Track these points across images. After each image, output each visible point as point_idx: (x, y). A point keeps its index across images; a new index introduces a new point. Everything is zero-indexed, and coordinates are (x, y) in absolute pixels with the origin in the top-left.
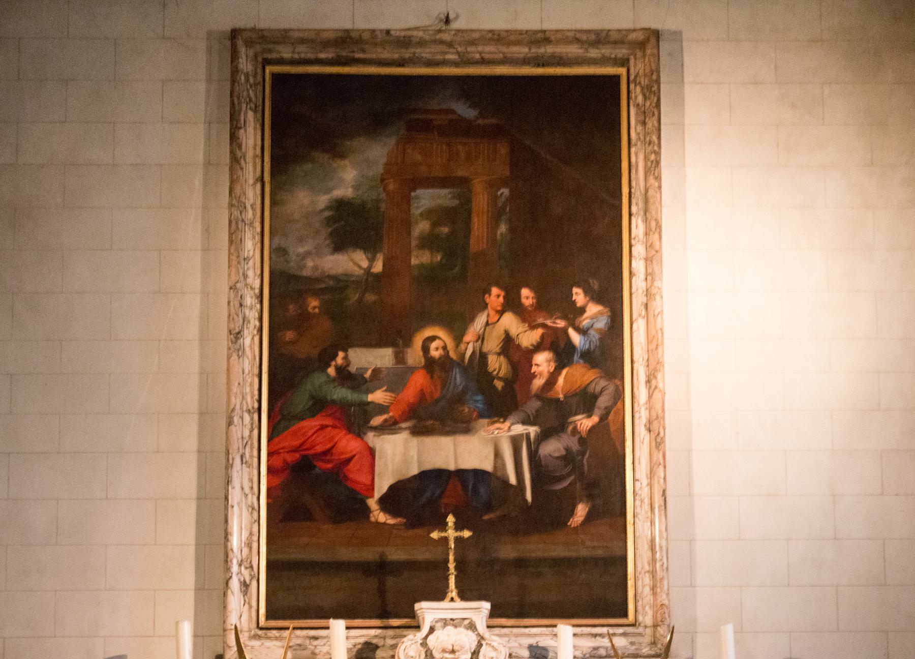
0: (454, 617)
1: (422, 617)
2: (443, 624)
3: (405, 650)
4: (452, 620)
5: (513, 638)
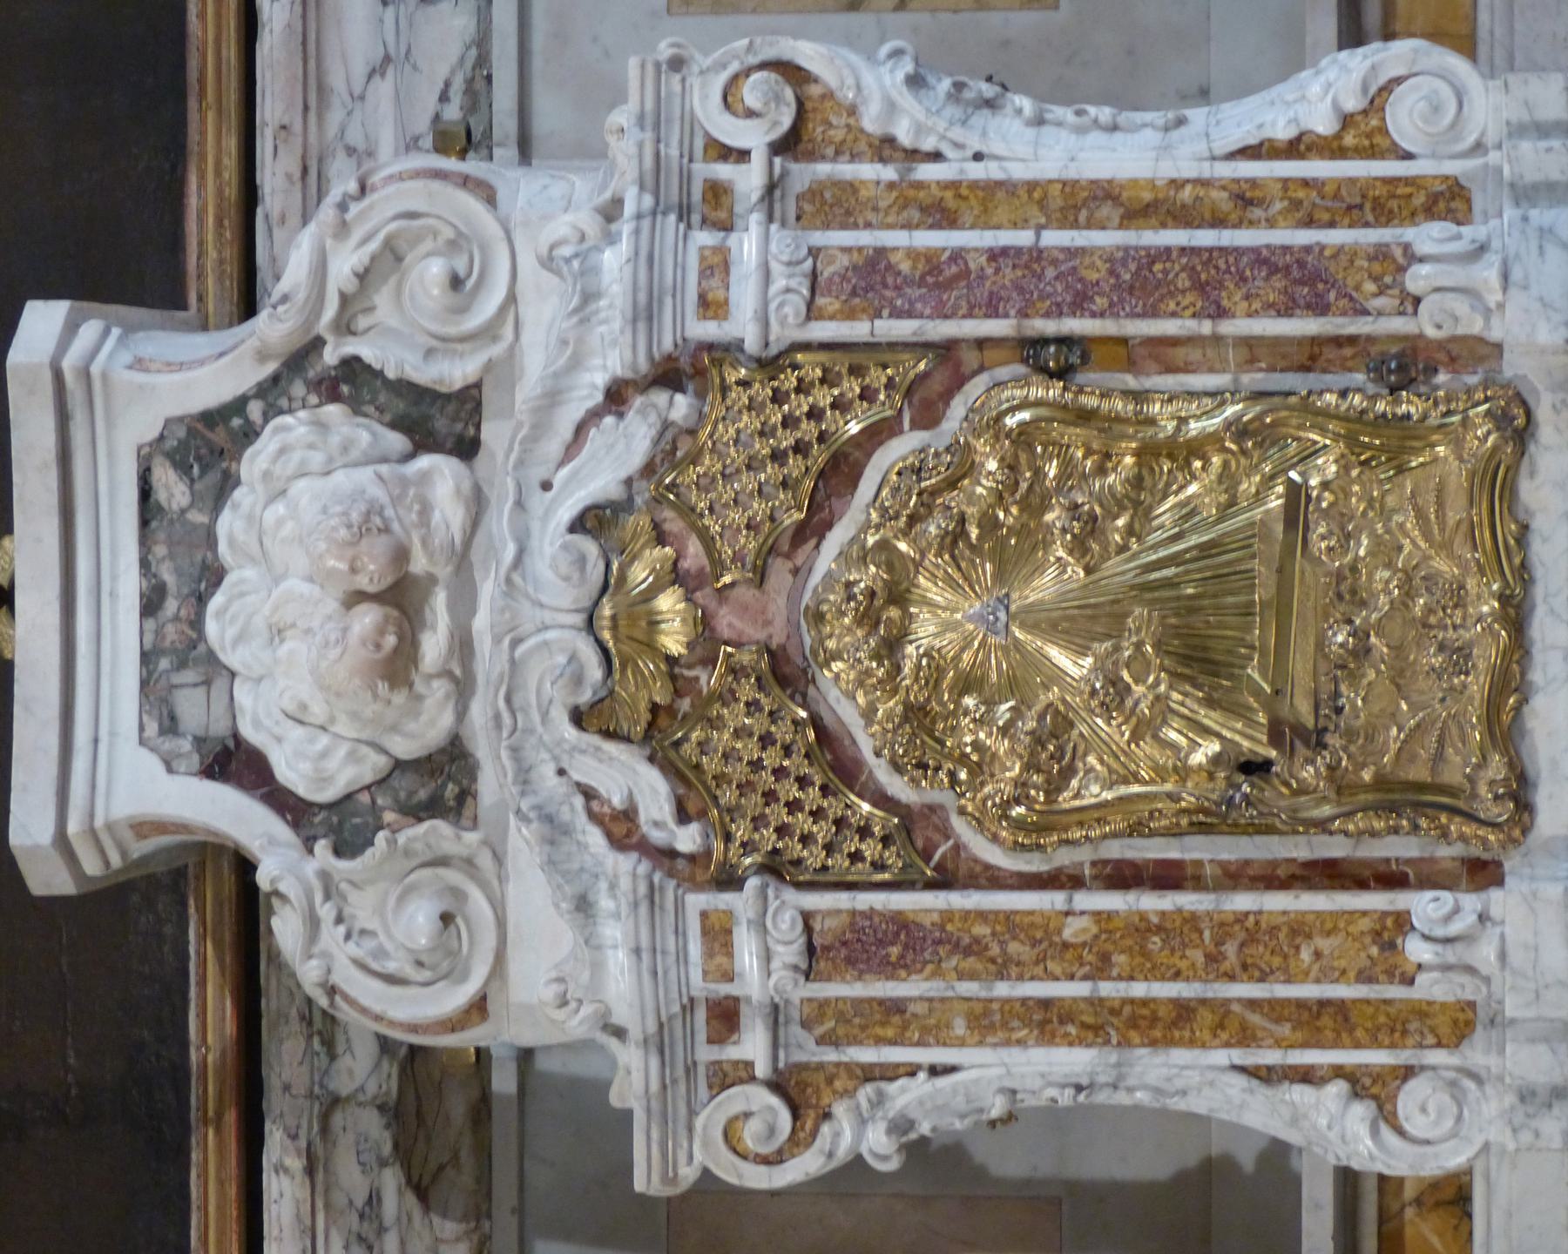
0: (129, 586)
1: (128, 835)
2: (189, 676)
3: (391, 979)
4: (150, 605)
5: (335, 117)
